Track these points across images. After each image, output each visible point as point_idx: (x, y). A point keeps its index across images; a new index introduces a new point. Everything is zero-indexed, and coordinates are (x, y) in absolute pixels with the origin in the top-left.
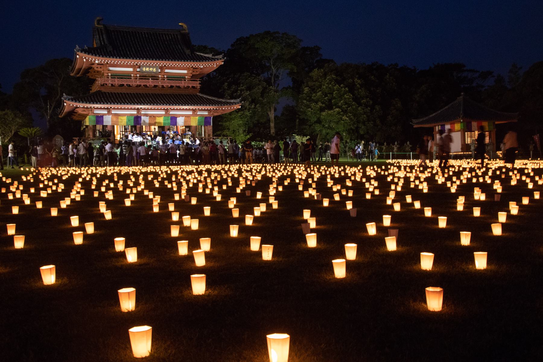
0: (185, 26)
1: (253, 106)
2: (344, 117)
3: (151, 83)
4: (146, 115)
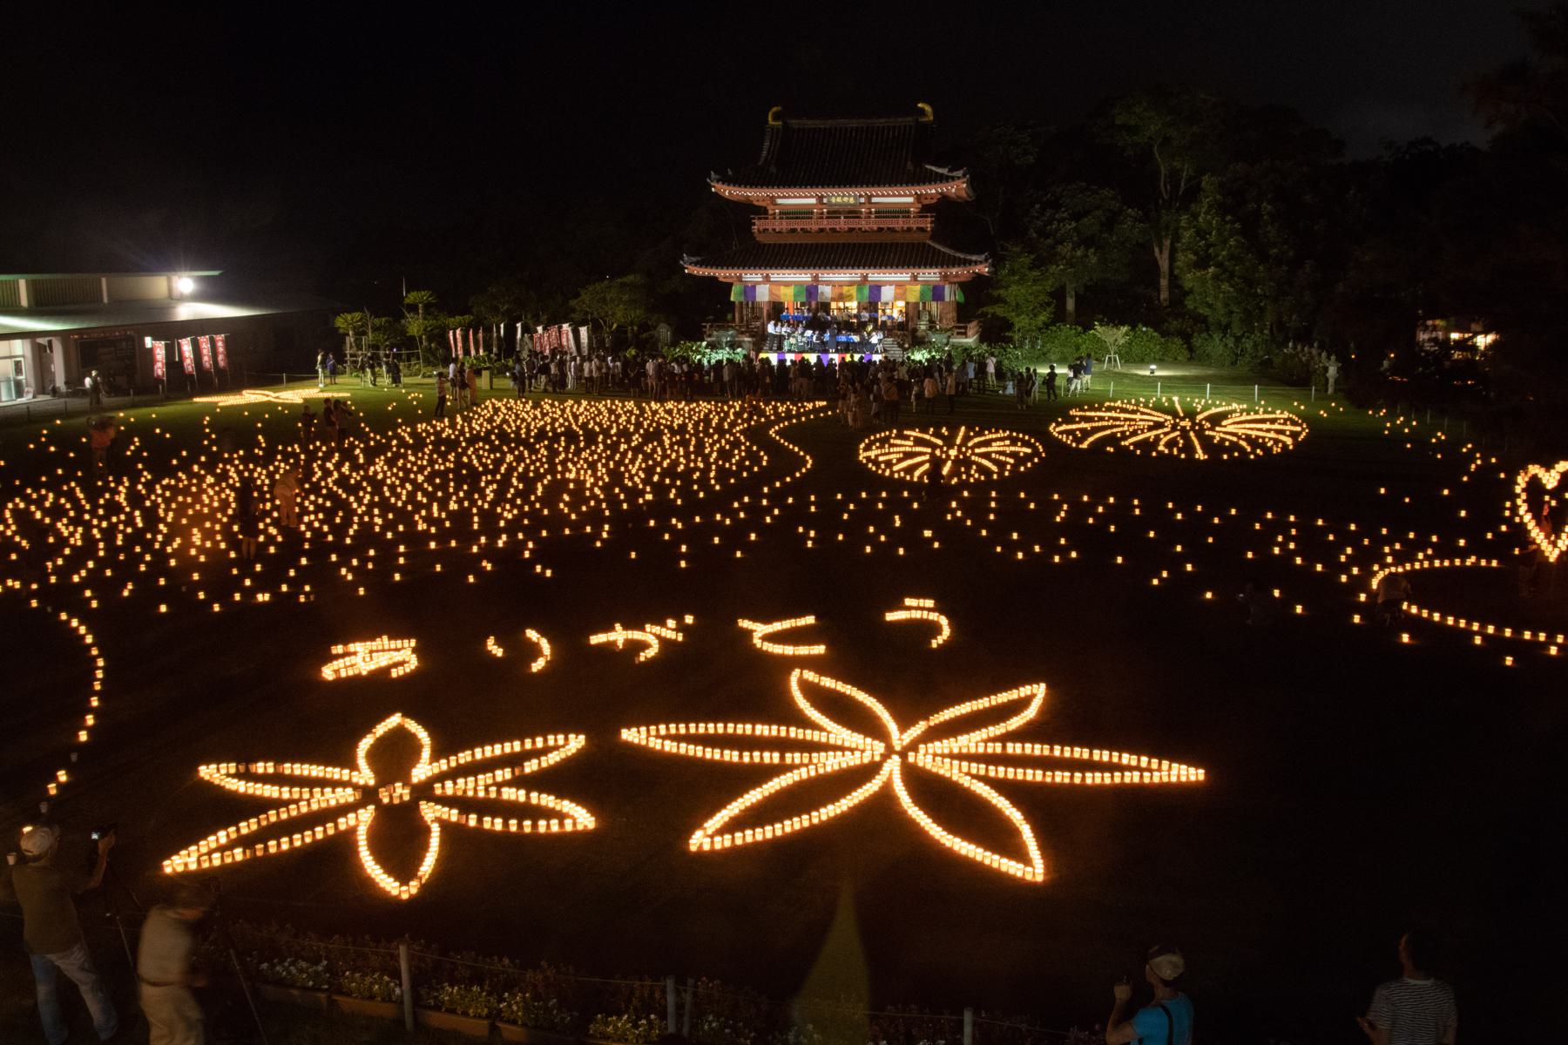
0: (928, 108)
1: (1079, 253)
2: (1225, 286)
3: (842, 224)
4: (827, 283)
